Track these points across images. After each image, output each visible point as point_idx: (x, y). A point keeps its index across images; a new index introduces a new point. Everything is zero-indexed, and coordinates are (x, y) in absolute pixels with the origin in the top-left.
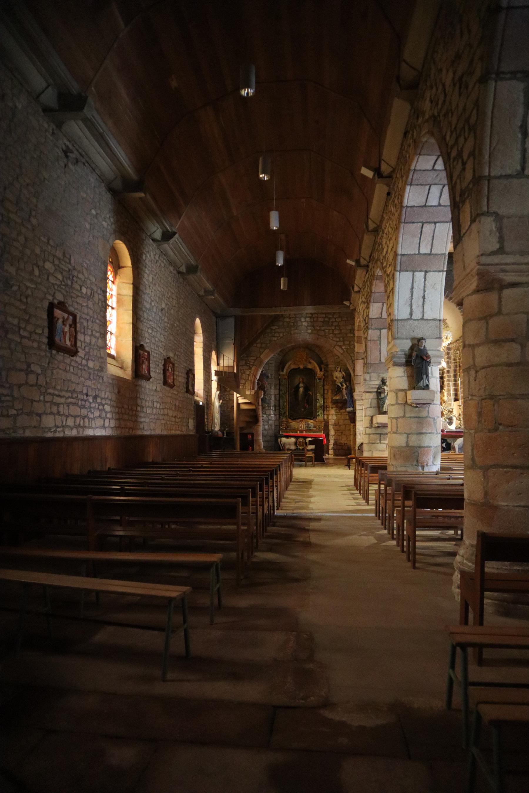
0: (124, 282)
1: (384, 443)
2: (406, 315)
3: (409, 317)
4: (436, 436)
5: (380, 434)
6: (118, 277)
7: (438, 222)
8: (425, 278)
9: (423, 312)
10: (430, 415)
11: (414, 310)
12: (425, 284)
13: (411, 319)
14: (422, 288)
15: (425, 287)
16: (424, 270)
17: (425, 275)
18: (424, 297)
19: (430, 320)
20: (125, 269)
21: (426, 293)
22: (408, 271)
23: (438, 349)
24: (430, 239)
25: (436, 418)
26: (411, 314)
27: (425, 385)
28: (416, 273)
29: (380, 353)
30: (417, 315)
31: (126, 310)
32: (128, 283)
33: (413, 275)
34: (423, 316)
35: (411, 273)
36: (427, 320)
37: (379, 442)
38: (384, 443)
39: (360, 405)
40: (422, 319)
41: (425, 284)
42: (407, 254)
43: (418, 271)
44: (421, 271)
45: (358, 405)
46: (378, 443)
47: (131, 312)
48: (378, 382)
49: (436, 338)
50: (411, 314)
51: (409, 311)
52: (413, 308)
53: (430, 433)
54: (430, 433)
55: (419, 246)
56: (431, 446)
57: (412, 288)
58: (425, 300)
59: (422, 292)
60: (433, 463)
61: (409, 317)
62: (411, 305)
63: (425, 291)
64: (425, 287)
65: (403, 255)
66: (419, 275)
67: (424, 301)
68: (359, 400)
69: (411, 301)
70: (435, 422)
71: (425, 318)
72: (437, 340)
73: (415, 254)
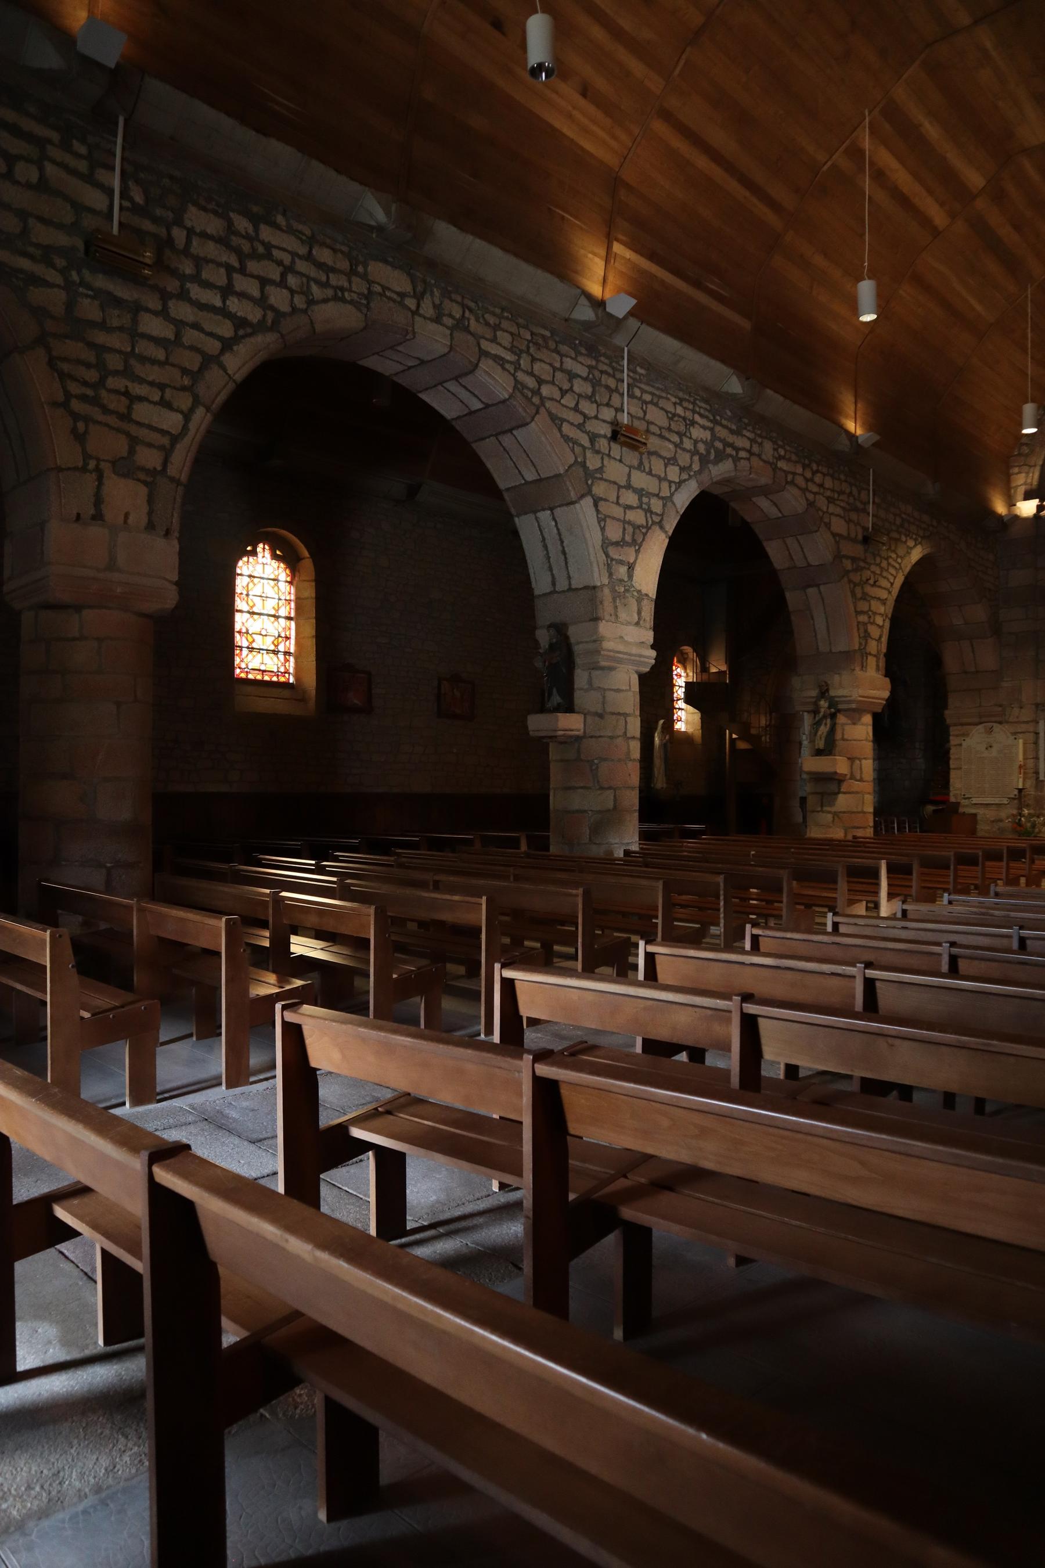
0: (304, 581)
1: (829, 812)
2: (548, 589)
3: (552, 589)
4: (599, 792)
5: (822, 794)
6: (297, 574)
7: (513, 429)
8: (554, 519)
9: (569, 578)
10: (583, 757)
11: (556, 576)
12: (558, 529)
13: (554, 592)
14: (557, 537)
15: (559, 534)
16: (546, 506)
17: (553, 513)
18: (564, 553)
19: (581, 589)
20: (303, 561)
21: (565, 544)
22: (526, 513)
23: (594, 637)
24: (524, 456)
25: (596, 761)
26: (554, 584)
27: (555, 704)
28: (539, 514)
29: (816, 636)
30: (562, 585)
31: (309, 618)
32: (308, 581)
33: (537, 519)
34: (570, 584)
35: (531, 516)
36: (577, 589)
37: (819, 809)
38: (829, 812)
39: (957, 736)
40: (570, 589)
41: (558, 529)
42: (512, 487)
43: (539, 511)
44: (544, 510)
45: (953, 735)
46: (818, 812)
47: (314, 621)
48: (814, 693)
49: (591, 620)
50: (554, 584)
51: (549, 579)
52: (554, 572)
53: (582, 788)
54: (582, 788)
55: (519, 471)
56: (585, 811)
57: (544, 539)
58: (567, 556)
59: (559, 542)
60: (590, 840)
61: (552, 589)
62: (551, 569)
63: (562, 542)
64: (559, 534)
65: (508, 489)
66: (545, 516)
67: (566, 558)
68: (955, 725)
69: (549, 562)
70: (594, 767)
71: (573, 587)
72: (591, 623)
73: (521, 485)
